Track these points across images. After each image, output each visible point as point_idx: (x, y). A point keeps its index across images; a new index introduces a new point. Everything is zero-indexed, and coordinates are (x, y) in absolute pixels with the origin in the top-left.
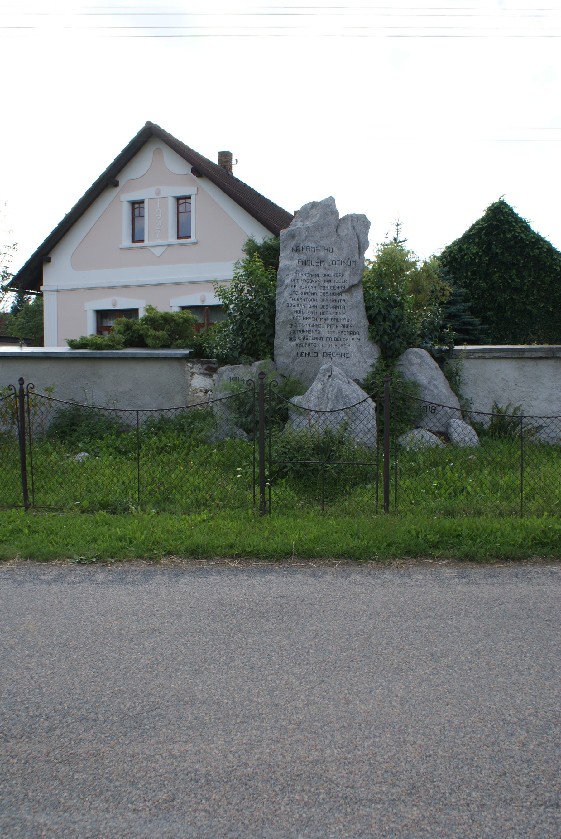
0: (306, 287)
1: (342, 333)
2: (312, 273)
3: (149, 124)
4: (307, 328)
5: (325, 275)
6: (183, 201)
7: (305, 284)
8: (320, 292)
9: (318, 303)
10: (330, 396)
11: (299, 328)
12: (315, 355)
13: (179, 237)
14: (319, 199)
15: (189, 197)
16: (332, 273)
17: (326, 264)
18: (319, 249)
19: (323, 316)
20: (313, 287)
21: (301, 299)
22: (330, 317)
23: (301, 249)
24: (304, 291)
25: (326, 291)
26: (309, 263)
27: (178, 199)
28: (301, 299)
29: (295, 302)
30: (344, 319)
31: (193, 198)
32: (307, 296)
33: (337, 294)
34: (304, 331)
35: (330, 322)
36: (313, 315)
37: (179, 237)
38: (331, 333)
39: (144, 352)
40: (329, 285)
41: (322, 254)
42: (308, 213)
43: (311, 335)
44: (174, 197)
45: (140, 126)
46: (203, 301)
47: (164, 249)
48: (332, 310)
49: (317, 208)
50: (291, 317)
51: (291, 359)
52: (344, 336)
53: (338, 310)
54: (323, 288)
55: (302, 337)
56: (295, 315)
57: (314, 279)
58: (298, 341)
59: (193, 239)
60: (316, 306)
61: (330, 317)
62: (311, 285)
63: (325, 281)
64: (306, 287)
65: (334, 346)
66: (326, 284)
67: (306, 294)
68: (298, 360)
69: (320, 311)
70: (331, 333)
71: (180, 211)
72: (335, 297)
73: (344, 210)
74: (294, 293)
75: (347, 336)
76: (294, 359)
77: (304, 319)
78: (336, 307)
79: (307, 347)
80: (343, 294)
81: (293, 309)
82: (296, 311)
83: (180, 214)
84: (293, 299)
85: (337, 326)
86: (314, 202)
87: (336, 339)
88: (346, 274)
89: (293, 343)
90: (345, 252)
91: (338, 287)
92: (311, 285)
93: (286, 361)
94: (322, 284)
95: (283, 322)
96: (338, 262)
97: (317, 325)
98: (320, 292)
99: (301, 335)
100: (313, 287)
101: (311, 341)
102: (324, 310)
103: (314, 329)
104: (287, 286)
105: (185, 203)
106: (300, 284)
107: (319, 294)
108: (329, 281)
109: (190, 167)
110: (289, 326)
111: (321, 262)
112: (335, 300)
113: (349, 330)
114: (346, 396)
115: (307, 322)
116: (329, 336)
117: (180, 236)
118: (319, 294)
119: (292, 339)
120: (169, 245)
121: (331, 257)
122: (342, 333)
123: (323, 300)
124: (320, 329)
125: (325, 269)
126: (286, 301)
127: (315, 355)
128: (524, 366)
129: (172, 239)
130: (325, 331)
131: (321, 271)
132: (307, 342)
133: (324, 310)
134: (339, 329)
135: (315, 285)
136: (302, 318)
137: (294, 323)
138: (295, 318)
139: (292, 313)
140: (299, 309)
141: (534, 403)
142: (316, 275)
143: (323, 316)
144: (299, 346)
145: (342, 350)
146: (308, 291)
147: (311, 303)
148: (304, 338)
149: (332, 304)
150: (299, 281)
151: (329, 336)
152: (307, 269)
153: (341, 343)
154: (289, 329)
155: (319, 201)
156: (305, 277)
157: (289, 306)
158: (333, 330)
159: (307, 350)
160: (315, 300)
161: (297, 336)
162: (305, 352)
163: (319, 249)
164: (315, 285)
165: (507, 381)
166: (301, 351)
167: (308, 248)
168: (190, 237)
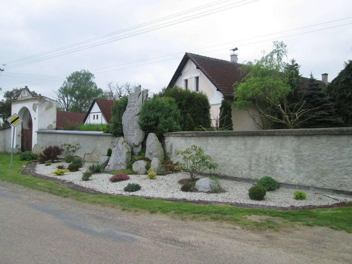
0: (128, 114)
1: (134, 128)
3: (186, 53)
4: (126, 127)
16: (135, 109)
20: (130, 114)
21: (126, 118)
22: (132, 123)
28: (126, 118)
40: (133, 113)
45: (184, 54)
69: (130, 121)
87: (132, 130)
91: (135, 114)
109: (196, 66)
114: (120, 148)
115: (126, 125)
124: (129, 127)
128: (187, 139)
134: (134, 127)
145: (133, 134)
147: (128, 119)
156: (128, 111)
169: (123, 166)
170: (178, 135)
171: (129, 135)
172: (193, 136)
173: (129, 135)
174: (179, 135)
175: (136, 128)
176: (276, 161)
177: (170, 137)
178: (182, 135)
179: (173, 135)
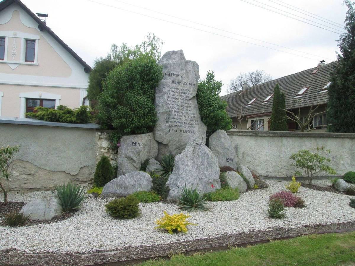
1: (190, 120)
2: (176, 88)
4: (176, 117)
5: (182, 90)
6: (30, 42)
7: (173, 93)
8: (180, 98)
9: (180, 104)
10: (200, 154)
11: (172, 117)
12: (179, 131)
13: (26, 61)
14: (176, 49)
15: (34, 41)
16: (185, 89)
17: (182, 84)
18: (179, 75)
19: (182, 111)
20: (177, 95)
22: (185, 111)
23: (171, 74)
24: (173, 96)
25: (183, 98)
26: (174, 83)
27: (27, 40)
28: (172, 101)
29: (169, 102)
30: (191, 113)
31: (37, 41)
32: (175, 100)
33: (188, 100)
34: (174, 118)
35: (185, 114)
36: (178, 110)
37: (26, 61)
38: (186, 120)
39: (38, 122)
40: (184, 95)
41: (180, 78)
42: (171, 56)
43: (178, 120)
44: (25, 39)
46: (40, 96)
47: (16, 66)
48: (186, 108)
49: (176, 55)
50: (168, 110)
51: (165, 133)
52: (191, 122)
53: (188, 109)
54: (181, 96)
55: (173, 122)
56: (170, 109)
57: (177, 91)
58: (170, 123)
59: (36, 63)
60: (179, 105)
61: (185, 111)
62: (176, 94)
63: (182, 93)
64: (174, 95)
65: (188, 127)
66: (182, 95)
67: (175, 98)
68: (169, 134)
69: (181, 108)
70: (186, 120)
71: (28, 47)
72: (187, 102)
73: (188, 57)
74: (169, 97)
75: (193, 122)
76: (167, 133)
77: (175, 112)
78: (187, 107)
79: (175, 127)
80: (190, 100)
81: (169, 106)
82: (171, 107)
83: (28, 49)
84: (169, 100)
85: (188, 117)
86: (174, 51)
87: (189, 124)
88: (191, 90)
89: (167, 124)
90: (190, 79)
92: (176, 94)
93: (162, 134)
94: (181, 94)
95: (162, 113)
96: (187, 84)
97: (180, 116)
98: (180, 98)
99: (173, 120)
100: (177, 95)
101: (178, 124)
102: (182, 108)
103: (179, 117)
104: (165, 93)
105: (31, 43)
106: (171, 93)
107: (180, 99)
108: (184, 93)
110: (166, 115)
111: (180, 82)
112: (187, 103)
113: (194, 119)
116: (185, 121)
117: (27, 60)
118: (180, 99)
119: (167, 122)
120: (20, 64)
121: (184, 81)
122: (190, 120)
123: (182, 103)
124: (181, 118)
125: (182, 86)
126: (166, 101)
127: (179, 131)
128: (257, 140)
129: (22, 61)
130: (183, 119)
131: (180, 87)
132: (176, 124)
133: (182, 108)
135: (178, 94)
136: (173, 111)
137: (169, 114)
138: (170, 111)
139: (169, 108)
140: (171, 106)
141: (261, 156)
142: (178, 89)
143: (182, 111)
144: (171, 126)
145: (191, 129)
146: (175, 97)
148: (174, 122)
149: (185, 105)
150: (171, 91)
151: (185, 121)
152: (174, 85)
153: (191, 126)
154: (165, 116)
155: (176, 50)
156: (173, 90)
157: (167, 104)
158: (187, 118)
159: (175, 128)
160: (178, 102)
161: (170, 121)
162: (174, 129)
163: (179, 75)
164: (178, 94)
165: (251, 146)
166: (172, 129)
167: (174, 75)
168: (33, 61)
169: (217, 183)
170: (248, 134)
171: (186, 132)
172: (269, 136)
173: (186, 132)
174: (250, 134)
175: (195, 121)
176: (340, 159)
177: (234, 137)
178: (254, 134)
179: (241, 134)
